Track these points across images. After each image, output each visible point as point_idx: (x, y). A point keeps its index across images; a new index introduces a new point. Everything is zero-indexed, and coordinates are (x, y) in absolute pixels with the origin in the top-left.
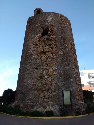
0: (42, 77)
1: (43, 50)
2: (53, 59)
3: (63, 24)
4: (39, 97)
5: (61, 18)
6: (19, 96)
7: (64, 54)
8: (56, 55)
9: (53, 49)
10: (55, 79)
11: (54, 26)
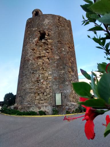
0: (38, 81)
1: (40, 54)
2: (49, 63)
3: (60, 26)
4: (36, 100)
5: (59, 20)
6: (18, 99)
7: (60, 58)
8: (52, 60)
9: (49, 54)
10: (51, 83)
11: (51, 30)
